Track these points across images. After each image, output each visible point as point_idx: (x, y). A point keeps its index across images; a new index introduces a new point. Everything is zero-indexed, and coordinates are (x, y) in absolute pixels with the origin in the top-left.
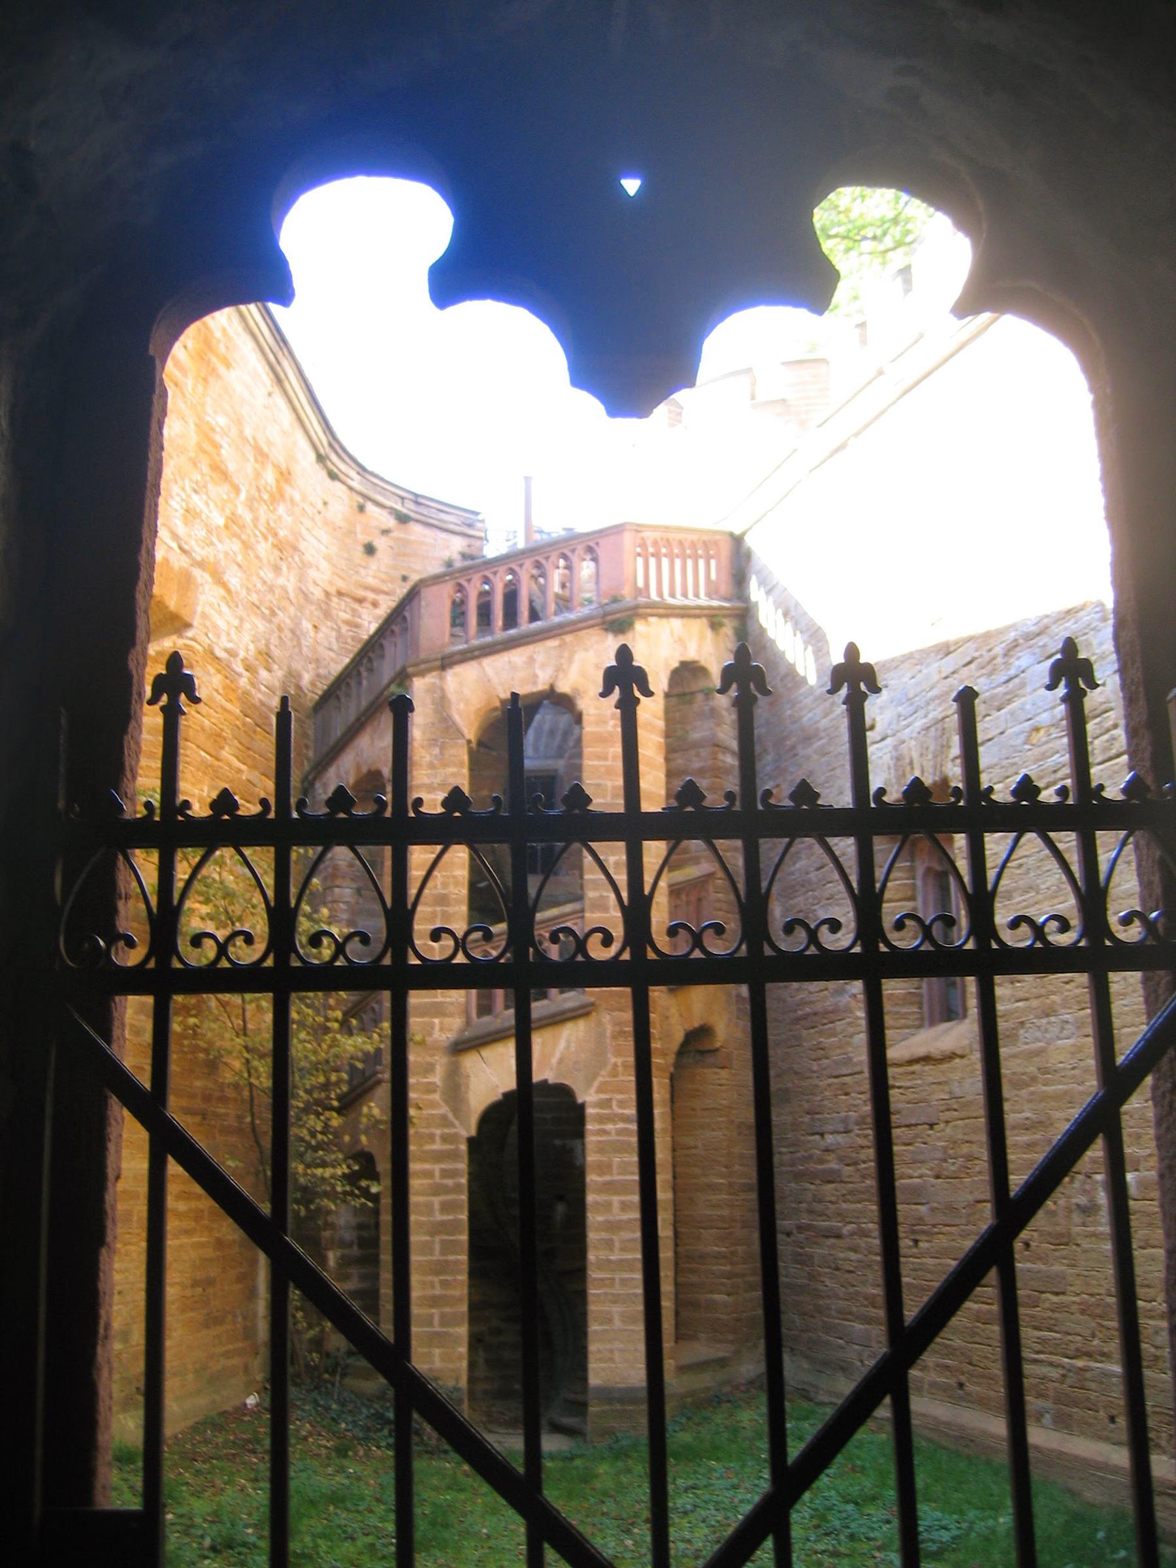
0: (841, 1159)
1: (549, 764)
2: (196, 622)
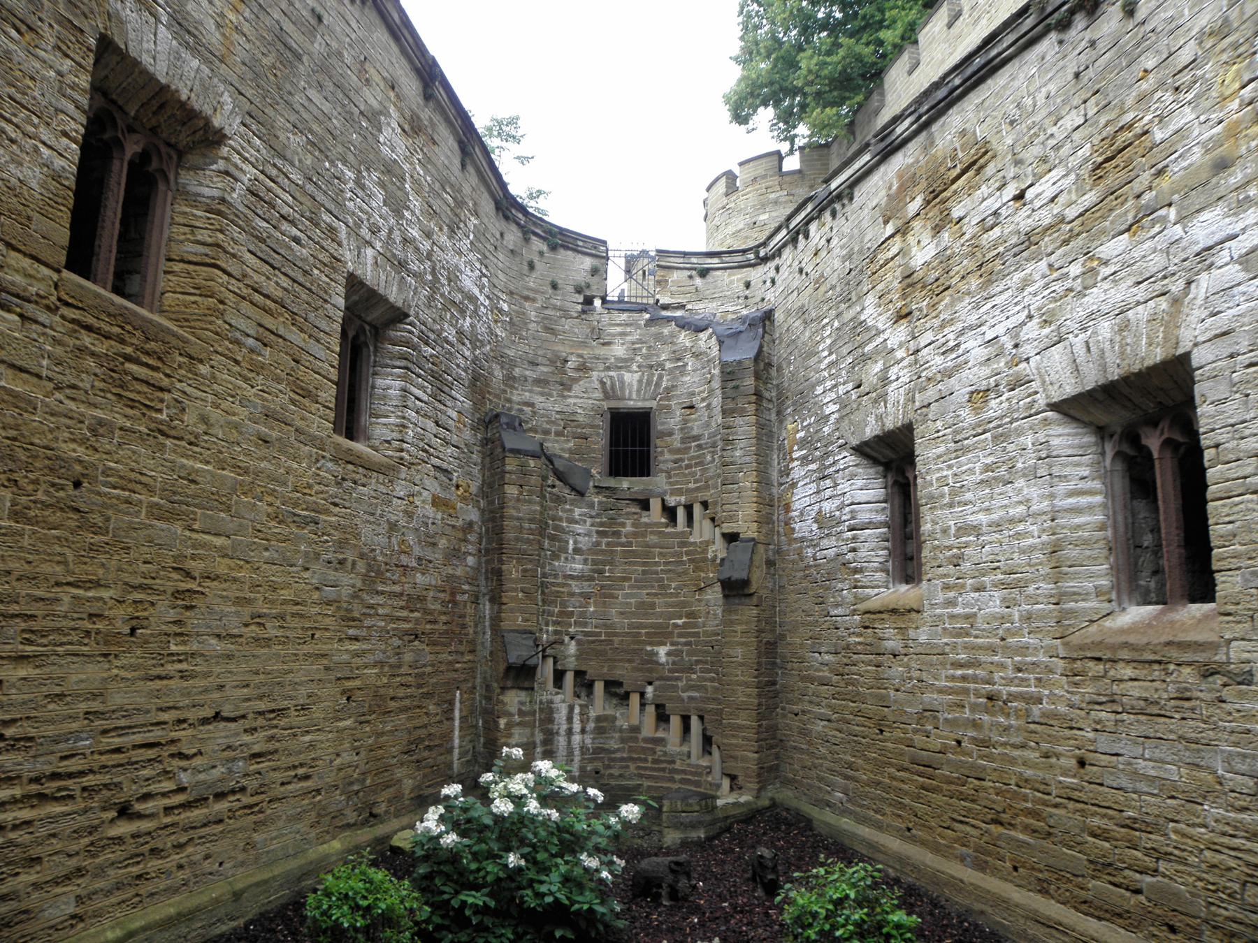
0: (831, 671)
1: (648, 404)
2: (412, 312)
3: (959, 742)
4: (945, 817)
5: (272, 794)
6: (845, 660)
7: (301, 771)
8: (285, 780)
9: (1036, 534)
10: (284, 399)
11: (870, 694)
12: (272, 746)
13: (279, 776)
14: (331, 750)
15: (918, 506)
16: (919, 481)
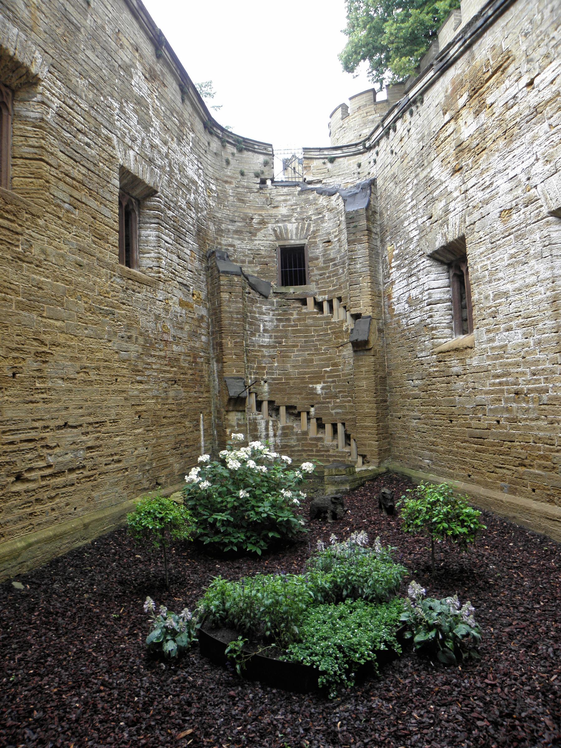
0: (420, 390)
1: (302, 242)
2: (159, 190)
3: (498, 422)
4: (491, 466)
5: (100, 470)
6: (428, 382)
7: (116, 458)
8: (107, 462)
9: (543, 292)
10: (89, 240)
11: (444, 400)
12: (98, 443)
13: (104, 460)
14: (132, 446)
15: (469, 285)
16: (470, 269)
